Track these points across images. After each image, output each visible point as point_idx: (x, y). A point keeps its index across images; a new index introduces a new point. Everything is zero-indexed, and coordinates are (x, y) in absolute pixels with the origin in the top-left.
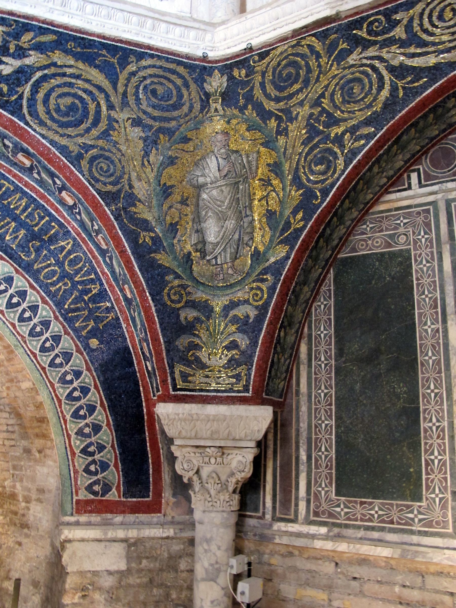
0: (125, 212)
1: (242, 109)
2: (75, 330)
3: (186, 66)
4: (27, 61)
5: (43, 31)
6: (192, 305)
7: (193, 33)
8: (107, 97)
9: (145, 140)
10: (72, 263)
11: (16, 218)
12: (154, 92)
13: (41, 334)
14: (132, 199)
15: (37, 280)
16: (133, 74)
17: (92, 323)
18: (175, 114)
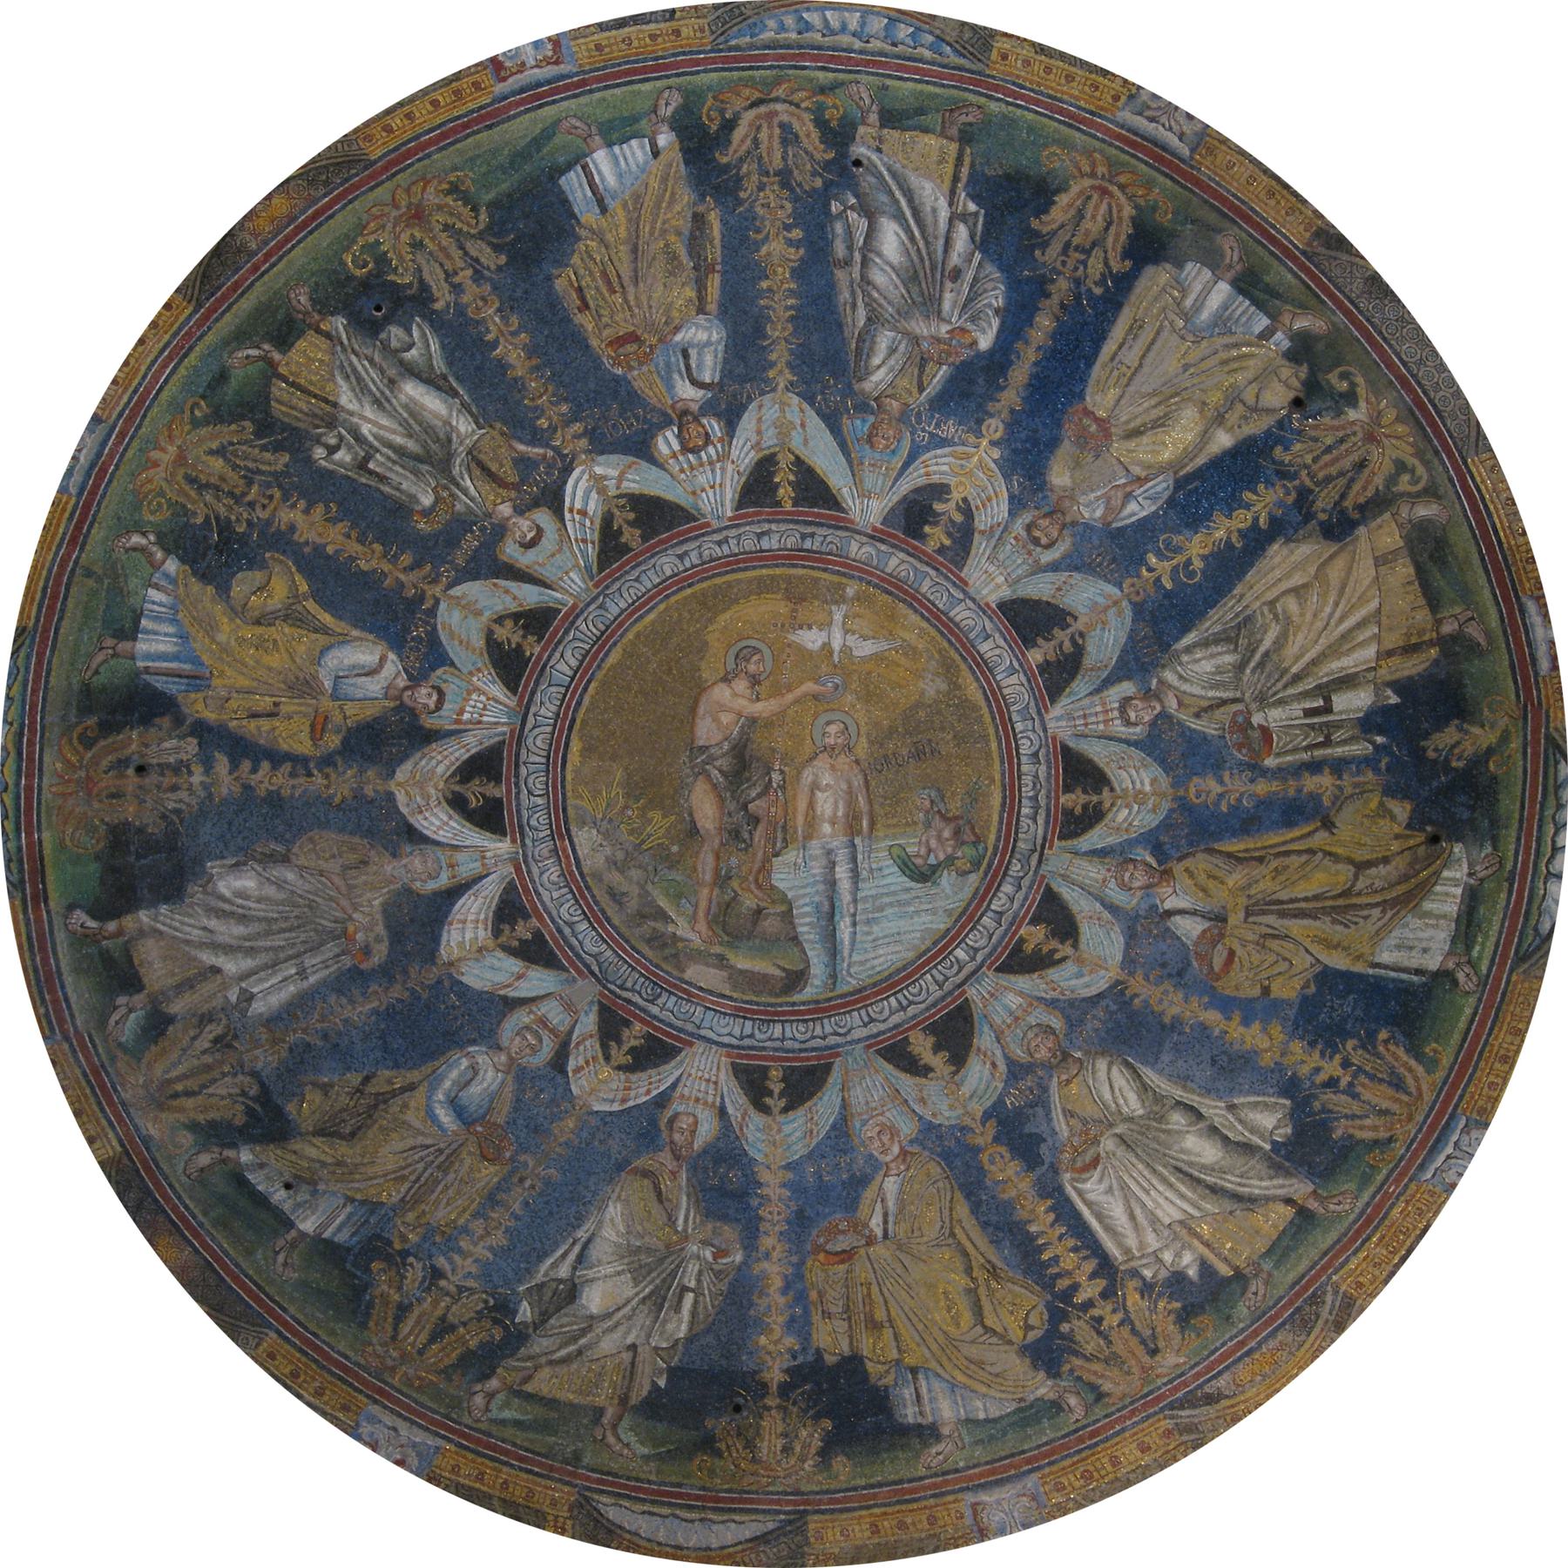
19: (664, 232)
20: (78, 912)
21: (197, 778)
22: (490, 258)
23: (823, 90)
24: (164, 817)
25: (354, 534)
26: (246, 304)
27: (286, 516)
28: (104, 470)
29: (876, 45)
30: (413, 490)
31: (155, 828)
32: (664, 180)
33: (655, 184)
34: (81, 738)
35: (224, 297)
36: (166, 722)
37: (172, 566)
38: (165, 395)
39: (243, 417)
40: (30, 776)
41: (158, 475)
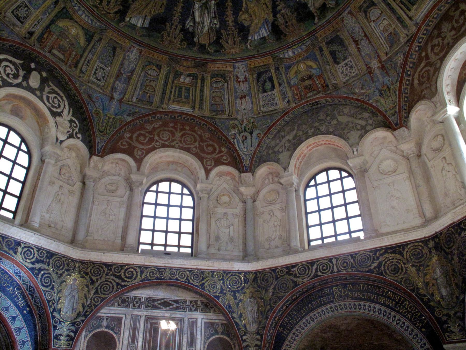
0: (418, 293)
1: (441, 252)
2: (417, 327)
3: (421, 242)
4: (380, 260)
5: (381, 250)
6: (444, 315)
7: (419, 232)
8: (403, 261)
9: (416, 270)
10: (410, 308)
11: (391, 299)
12: (415, 254)
13: (408, 330)
14: (418, 289)
15: (402, 315)
16: (407, 251)
17: (421, 324)
18: (423, 259)
19: (140, 4)
20: (315, 22)
21: (283, 11)
22: (168, 25)
23: (97, 7)
24: (293, 14)
25: (227, 10)
26: (202, 56)
27: (231, 24)
28: (241, 59)
29: (83, 9)
30: (213, 6)
31: (295, 14)
32: (133, 12)
33: (135, 13)
34: (285, 37)
35: (204, 60)
36: (276, 23)
37: (250, 38)
38: (224, 58)
39: (220, 43)
40: (295, 43)
41: (237, 50)
